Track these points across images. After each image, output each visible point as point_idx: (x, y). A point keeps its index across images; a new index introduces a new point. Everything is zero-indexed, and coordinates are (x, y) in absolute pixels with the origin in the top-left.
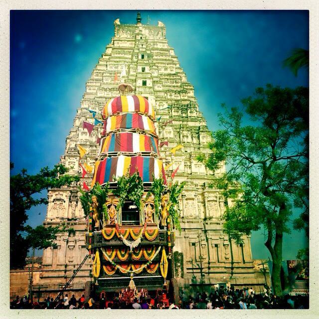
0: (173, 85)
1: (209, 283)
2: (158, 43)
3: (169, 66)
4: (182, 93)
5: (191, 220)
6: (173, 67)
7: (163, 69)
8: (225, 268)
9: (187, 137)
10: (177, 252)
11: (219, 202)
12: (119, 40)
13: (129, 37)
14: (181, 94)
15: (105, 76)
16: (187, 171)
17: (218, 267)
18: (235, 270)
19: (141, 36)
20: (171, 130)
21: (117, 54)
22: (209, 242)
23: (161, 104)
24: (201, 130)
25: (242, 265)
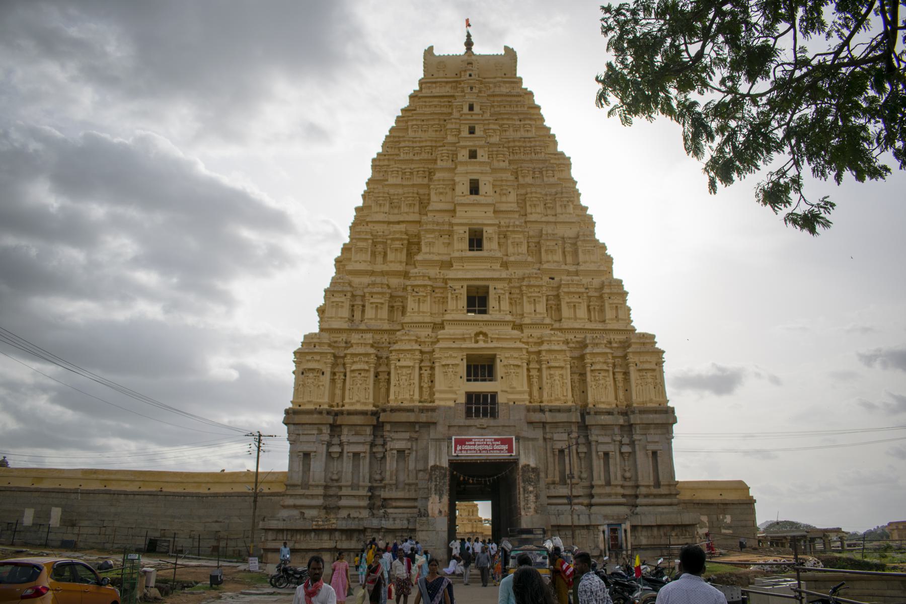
6: (530, 125)
7: (511, 129)
11: (614, 374)
14: (544, 173)
17: (609, 495)
18: (639, 501)
20: (522, 240)
22: (594, 447)
24: (581, 238)
25: (654, 491)
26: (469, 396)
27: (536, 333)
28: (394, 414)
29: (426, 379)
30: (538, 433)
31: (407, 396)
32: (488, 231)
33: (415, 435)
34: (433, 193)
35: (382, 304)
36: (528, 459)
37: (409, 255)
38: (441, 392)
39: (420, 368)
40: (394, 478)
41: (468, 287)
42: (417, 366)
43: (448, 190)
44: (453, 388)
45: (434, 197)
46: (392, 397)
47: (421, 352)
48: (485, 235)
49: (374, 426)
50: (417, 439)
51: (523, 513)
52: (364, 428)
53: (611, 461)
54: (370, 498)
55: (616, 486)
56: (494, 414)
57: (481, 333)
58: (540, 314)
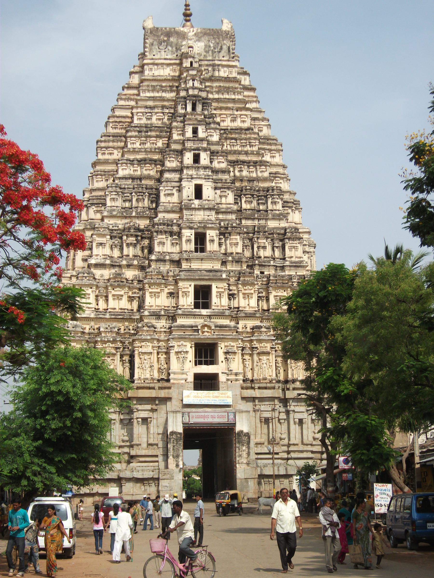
0: (246, 149)
1: (285, 473)
2: (220, 68)
3: (239, 113)
4: (260, 166)
5: (264, 385)
6: (246, 115)
7: (229, 119)
8: (312, 452)
9: (264, 248)
10: (242, 431)
12: (153, 64)
14: (258, 167)
15: (131, 137)
16: (262, 306)
17: (302, 452)
19: (190, 60)
21: (149, 91)
22: (291, 415)
23: (224, 194)
24: (289, 235)
27: (251, 323)
28: (140, 391)
29: (163, 362)
30: (249, 406)
31: (148, 376)
32: (211, 234)
33: (154, 407)
34: (162, 194)
35: (122, 296)
36: (242, 426)
38: (174, 373)
39: (158, 353)
41: (195, 286)
42: (156, 351)
43: (174, 191)
45: (163, 199)
46: (136, 376)
48: (208, 238)
50: (156, 410)
51: (237, 465)
53: (304, 426)
55: (307, 445)
57: (206, 326)
58: (252, 307)
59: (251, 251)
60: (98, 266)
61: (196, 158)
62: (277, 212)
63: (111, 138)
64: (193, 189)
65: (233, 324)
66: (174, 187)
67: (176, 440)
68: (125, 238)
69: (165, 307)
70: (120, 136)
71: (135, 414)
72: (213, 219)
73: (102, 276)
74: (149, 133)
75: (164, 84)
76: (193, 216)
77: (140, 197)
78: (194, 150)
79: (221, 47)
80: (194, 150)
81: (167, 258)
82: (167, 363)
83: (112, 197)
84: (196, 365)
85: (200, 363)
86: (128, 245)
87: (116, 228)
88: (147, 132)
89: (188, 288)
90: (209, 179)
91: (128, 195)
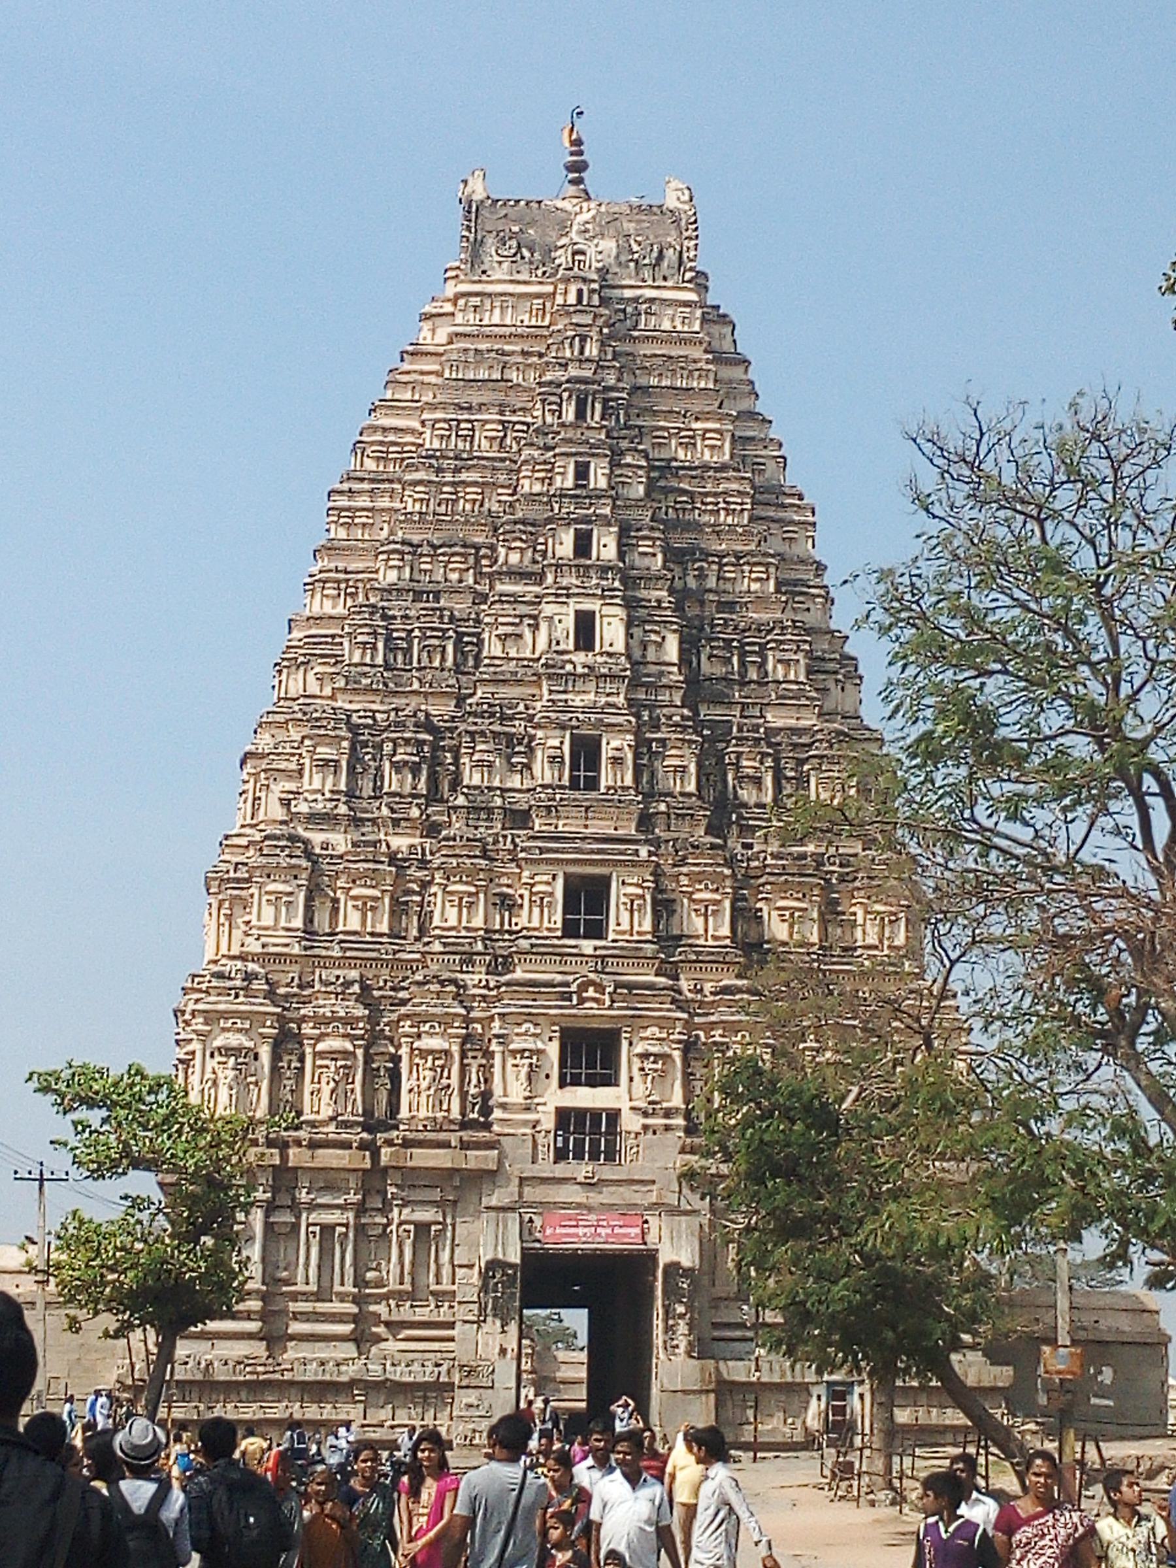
13: (524, 277)
26: (563, 1115)
32: (613, 744)
37: (434, 781)
38: (503, 1106)
39: (463, 1055)
40: (407, 1279)
42: (455, 1049)
44: (530, 1094)
45: (493, 648)
46: (404, 1113)
47: (467, 1021)
48: (606, 752)
49: (364, 1171)
50: (455, 1202)
52: (343, 1175)
54: (355, 1319)
56: (611, 1155)
57: (592, 983)
58: (715, 938)
59: (719, 786)
60: (315, 819)
61: (583, 545)
62: (795, 687)
63: (366, 486)
64: (570, 622)
65: (662, 980)
66: (521, 617)
67: (502, 1282)
68: (388, 748)
69: (487, 931)
70: (391, 481)
71: (396, 1210)
72: (620, 700)
73: (325, 846)
74: (464, 476)
75: (507, 348)
76: (569, 696)
77: (436, 642)
78: (576, 521)
79: (661, 252)
80: (576, 521)
81: (498, 801)
82: (486, 1081)
83: (360, 639)
84: (562, 1085)
85: (576, 1082)
86: (397, 767)
87: (370, 721)
88: (457, 470)
89: (548, 883)
90: (612, 597)
91: (403, 635)
